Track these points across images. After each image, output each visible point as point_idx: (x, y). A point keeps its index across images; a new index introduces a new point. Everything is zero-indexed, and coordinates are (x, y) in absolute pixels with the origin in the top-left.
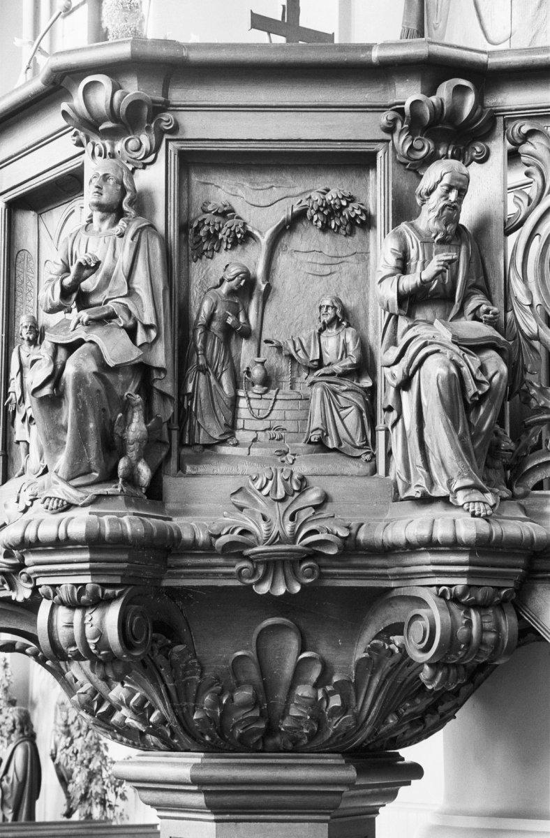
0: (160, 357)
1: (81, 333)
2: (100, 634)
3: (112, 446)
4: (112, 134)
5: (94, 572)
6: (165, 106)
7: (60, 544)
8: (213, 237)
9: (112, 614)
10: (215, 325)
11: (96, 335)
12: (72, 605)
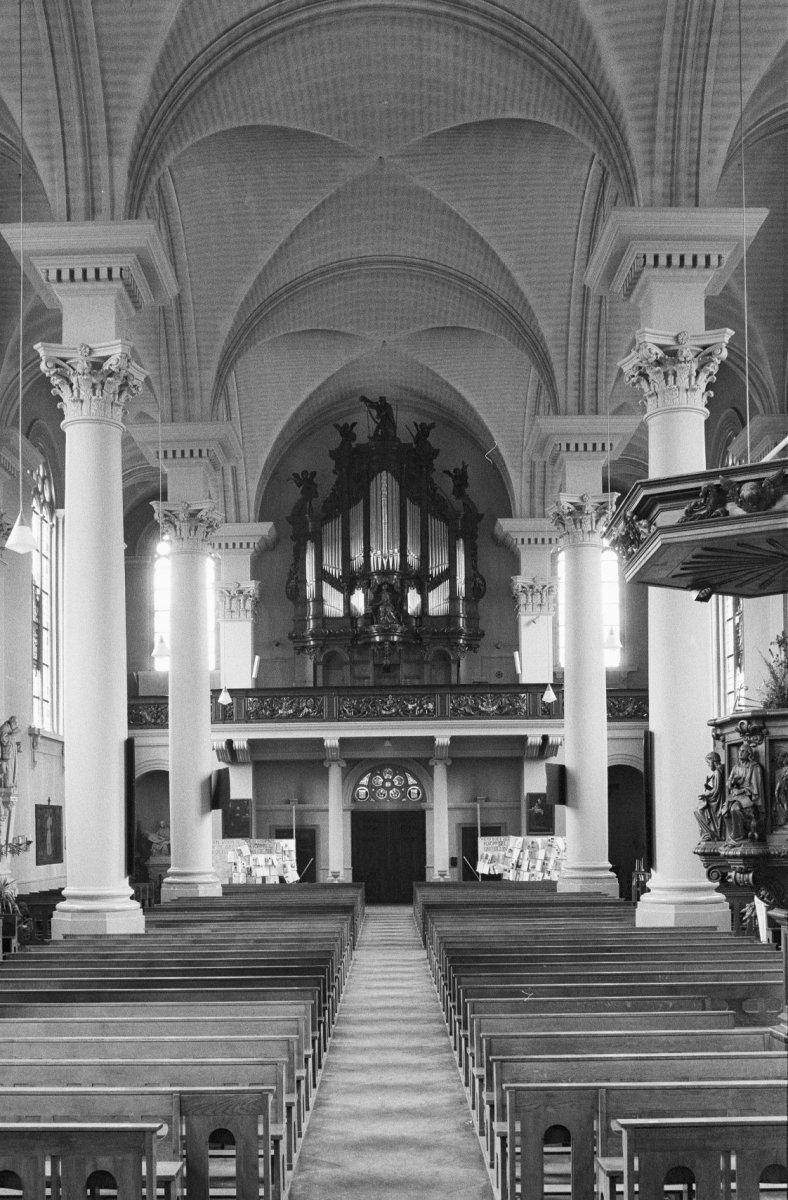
0: (760, 803)
1: (735, 798)
2: (748, 880)
3: (746, 829)
4: (750, 736)
5: (744, 864)
6: (765, 727)
7: (735, 857)
8: (781, 763)
9: (751, 875)
10: (782, 790)
11: (739, 799)
12: (741, 873)
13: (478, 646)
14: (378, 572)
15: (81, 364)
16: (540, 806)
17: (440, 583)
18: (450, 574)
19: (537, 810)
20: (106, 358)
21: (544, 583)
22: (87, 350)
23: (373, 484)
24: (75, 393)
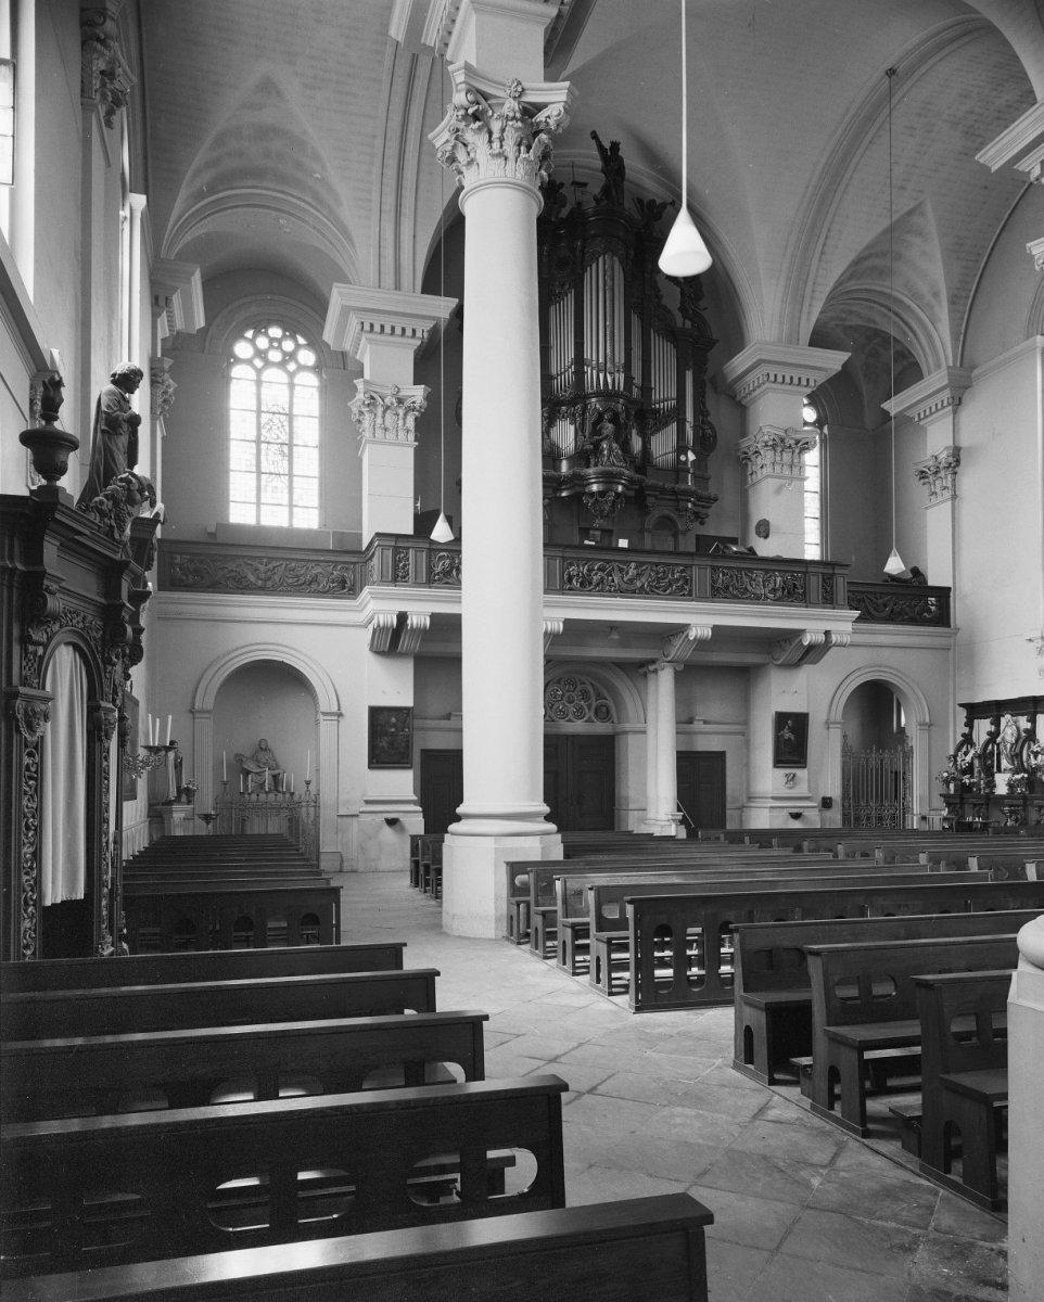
13: (707, 516)
14: (597, 394)
15: (510, 106)
16: (792, 730)
17: (666, 425)
18: (677, 414)
19: (787, 735)
20: (543, 106)
21: (798, 436)
22: (520, 89)
23: (587, 276)
24: (496, 145)
